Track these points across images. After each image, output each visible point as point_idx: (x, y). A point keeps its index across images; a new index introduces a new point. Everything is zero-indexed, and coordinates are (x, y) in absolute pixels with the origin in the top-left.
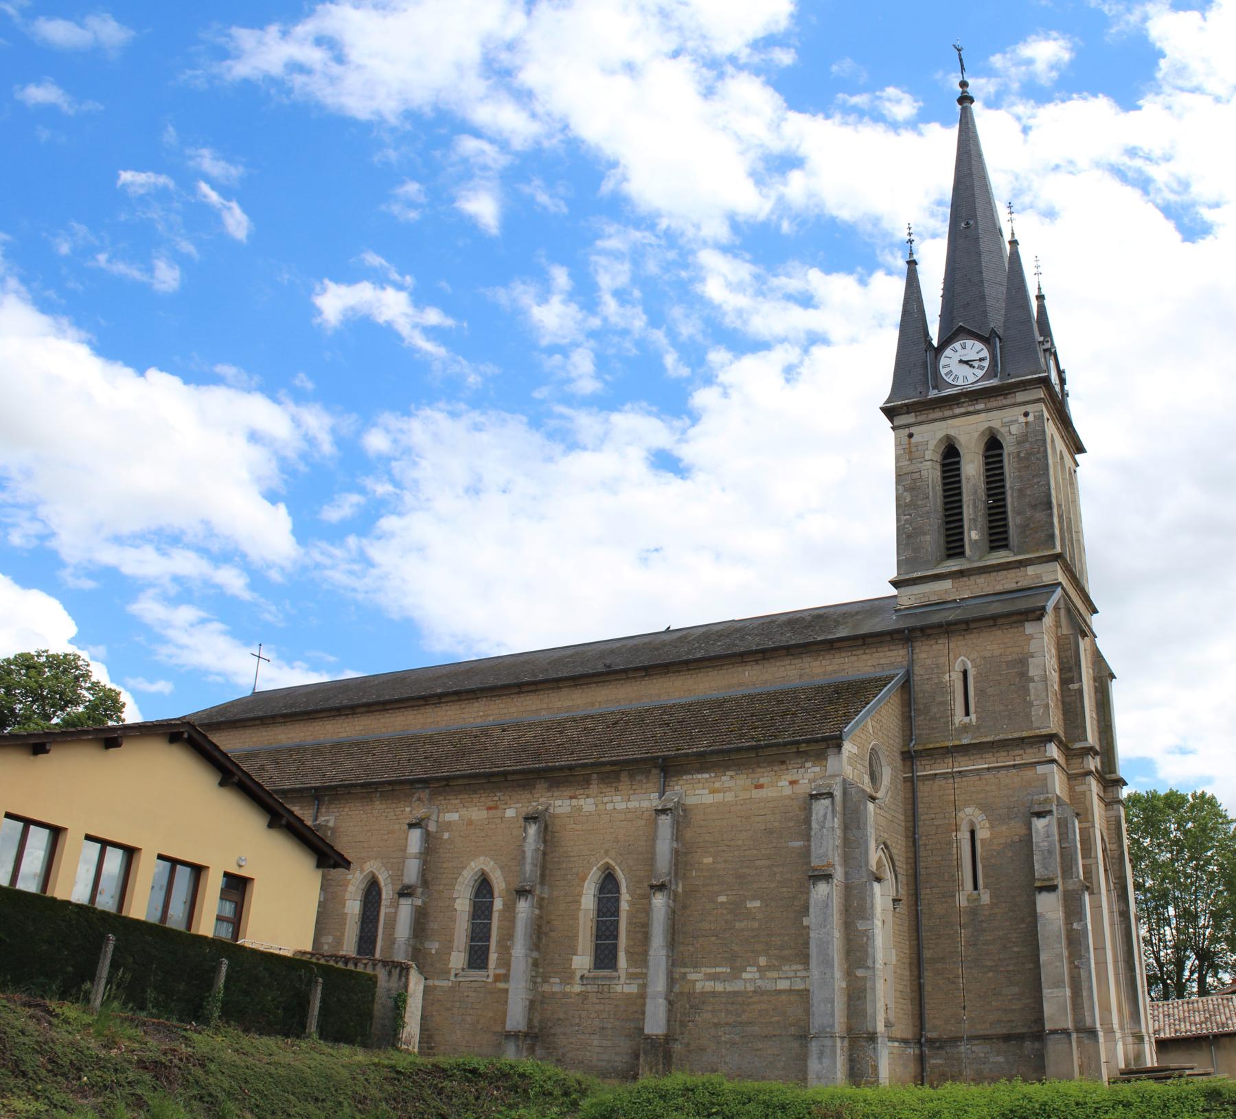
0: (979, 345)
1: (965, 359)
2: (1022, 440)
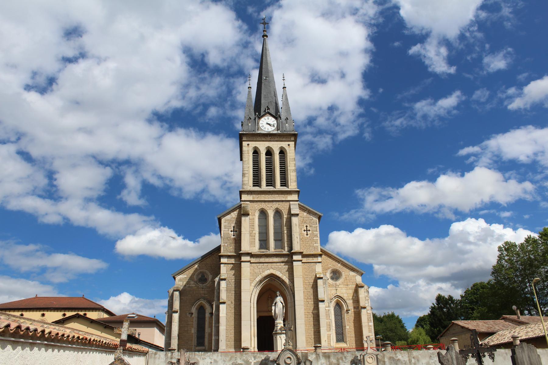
0: (273, 119)
1: (268, 123)
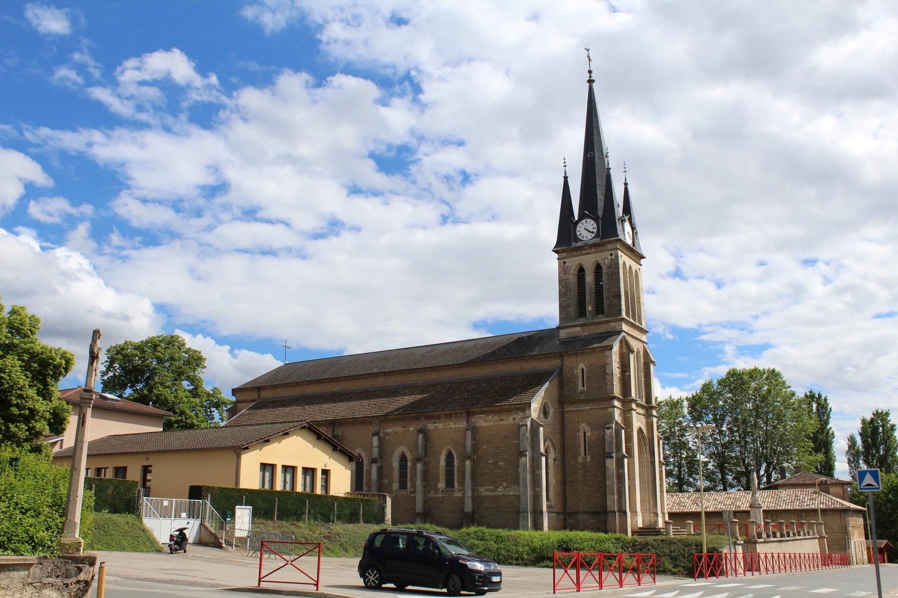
2: (609, 267)
